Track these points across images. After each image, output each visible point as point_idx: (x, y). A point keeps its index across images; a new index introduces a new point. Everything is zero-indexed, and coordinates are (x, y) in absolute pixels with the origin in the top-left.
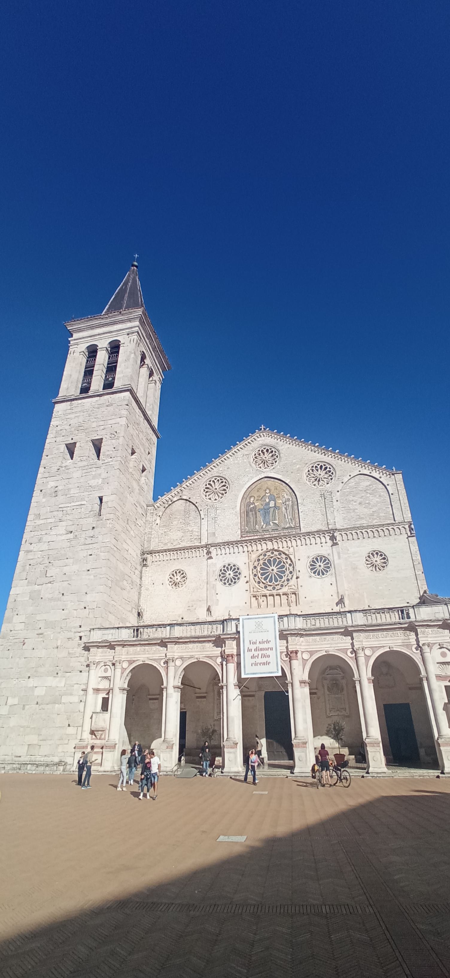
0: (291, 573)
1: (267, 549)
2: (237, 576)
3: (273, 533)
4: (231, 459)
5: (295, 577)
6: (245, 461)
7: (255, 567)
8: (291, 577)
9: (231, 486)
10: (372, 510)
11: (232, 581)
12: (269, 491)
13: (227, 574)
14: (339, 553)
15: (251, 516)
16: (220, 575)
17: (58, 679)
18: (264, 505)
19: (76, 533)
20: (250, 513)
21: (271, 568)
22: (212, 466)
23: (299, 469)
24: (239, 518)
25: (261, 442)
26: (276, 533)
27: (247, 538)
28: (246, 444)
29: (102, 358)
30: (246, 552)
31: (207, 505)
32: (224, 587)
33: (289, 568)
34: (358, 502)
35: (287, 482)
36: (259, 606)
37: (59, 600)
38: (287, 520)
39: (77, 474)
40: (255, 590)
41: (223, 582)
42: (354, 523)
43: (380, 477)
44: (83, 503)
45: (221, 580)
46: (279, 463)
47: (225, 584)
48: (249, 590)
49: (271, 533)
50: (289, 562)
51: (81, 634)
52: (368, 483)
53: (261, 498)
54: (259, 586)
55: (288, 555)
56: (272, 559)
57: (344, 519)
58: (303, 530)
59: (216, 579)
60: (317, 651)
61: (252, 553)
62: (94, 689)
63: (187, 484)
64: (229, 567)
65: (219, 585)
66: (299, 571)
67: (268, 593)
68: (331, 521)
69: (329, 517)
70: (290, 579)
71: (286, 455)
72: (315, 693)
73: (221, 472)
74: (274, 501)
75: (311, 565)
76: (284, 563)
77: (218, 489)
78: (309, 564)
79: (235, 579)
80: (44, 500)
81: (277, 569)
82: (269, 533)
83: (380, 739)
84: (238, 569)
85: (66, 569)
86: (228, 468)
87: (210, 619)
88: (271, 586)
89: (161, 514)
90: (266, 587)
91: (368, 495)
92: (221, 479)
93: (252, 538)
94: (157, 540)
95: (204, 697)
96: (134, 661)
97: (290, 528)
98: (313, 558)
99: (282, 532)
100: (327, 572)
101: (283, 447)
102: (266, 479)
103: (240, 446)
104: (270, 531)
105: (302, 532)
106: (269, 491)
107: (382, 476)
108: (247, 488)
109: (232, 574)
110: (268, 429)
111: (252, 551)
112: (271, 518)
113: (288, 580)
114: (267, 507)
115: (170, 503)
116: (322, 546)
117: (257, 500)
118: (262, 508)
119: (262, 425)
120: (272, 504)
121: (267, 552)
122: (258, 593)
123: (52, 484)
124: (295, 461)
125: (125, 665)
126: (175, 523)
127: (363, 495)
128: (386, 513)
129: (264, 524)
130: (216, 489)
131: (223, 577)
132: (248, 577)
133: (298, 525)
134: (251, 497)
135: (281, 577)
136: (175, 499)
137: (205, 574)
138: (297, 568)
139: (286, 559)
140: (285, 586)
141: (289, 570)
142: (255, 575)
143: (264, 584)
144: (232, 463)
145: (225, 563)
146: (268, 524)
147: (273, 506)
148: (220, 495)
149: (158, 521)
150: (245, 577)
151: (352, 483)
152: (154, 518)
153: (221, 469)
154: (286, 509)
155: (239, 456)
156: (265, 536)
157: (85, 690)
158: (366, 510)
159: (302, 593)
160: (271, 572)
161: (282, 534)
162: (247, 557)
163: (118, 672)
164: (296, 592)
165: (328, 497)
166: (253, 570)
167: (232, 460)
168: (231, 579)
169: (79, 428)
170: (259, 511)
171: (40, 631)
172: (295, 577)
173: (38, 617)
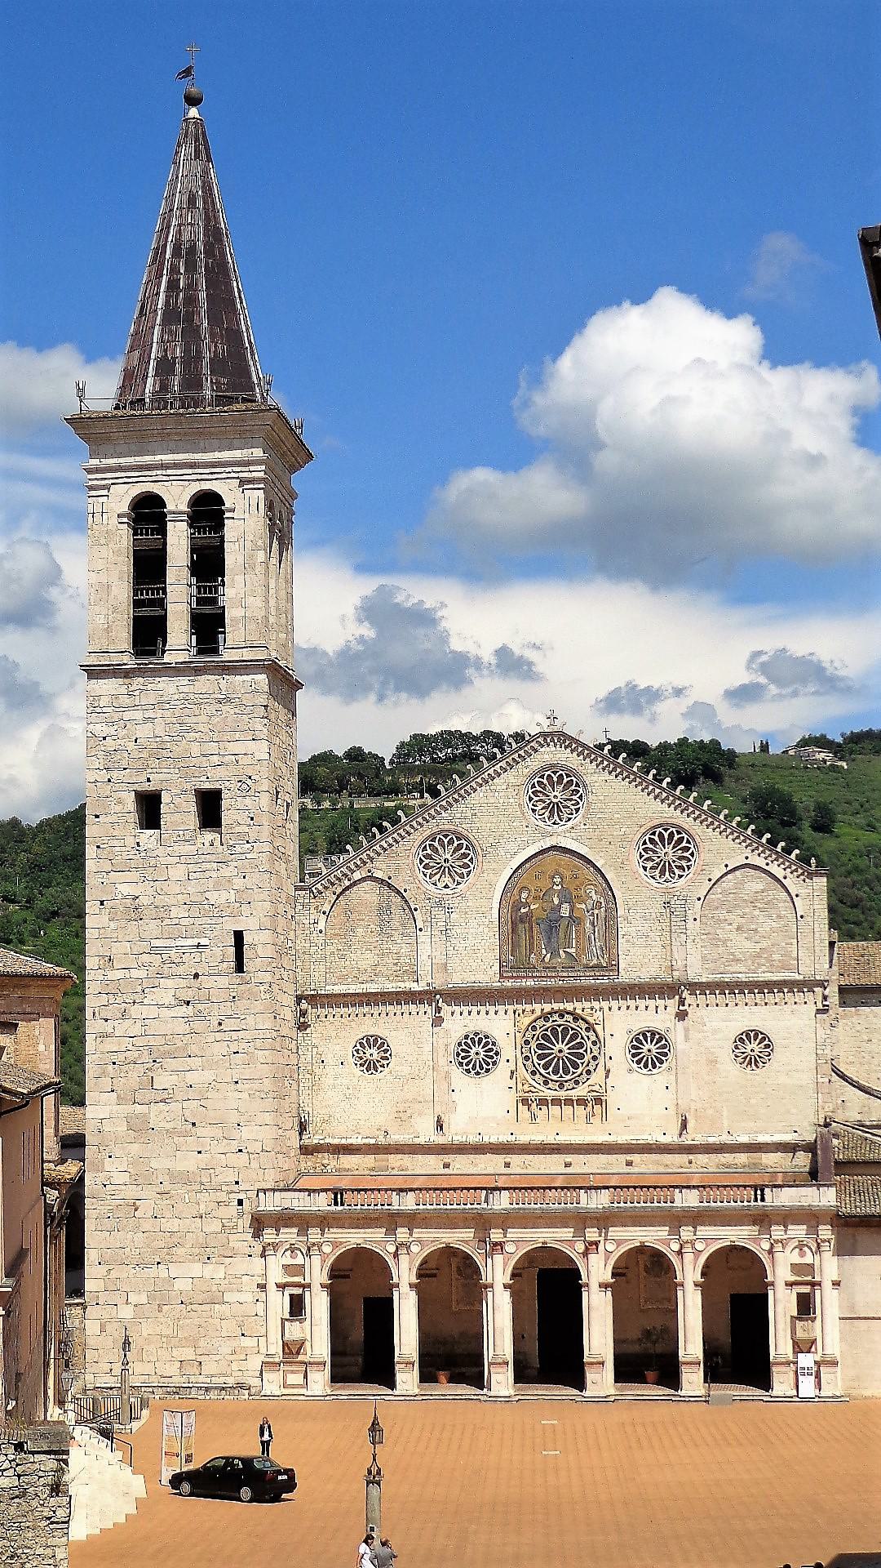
0: (595, 1058)
3: (565, 974)
4: (481, 792)
5: (601, 1071)
7: (527, 1042)
10: (759, 946)
11: (481, 1067)
12: (559, 880)
13: (473, 1051)
14: (687, 1030)
17: (210, 1267)
20: (520, 926)
32: (466, 1079)
34: (735, 925)
36: (534, 1117)
40: (526, 1088)
41: (465, 1067)
42: (721, 970)
43: (785, 878)
44: (204, 941)
45: (461, 1064)
48: (514, 1088)
50: (593, 1038)
51: (242, 1196)
52: (760, 887)
56: (559, 1030)
58: (626, 976)
59: (451, 1062)
60: (627, 1240)
62: (278, 1286)
63: (383, 843)
65: (457, 1073)
66: (611, 1058)
67: (549, 1094)
69: (676, 956)
76: (582, 1038)
77: (450, 858)
80: (113, 925)
81: (569, 1049)
83: (701, 1357)
84: (494, 1044)
85: (190, 1078)
89: (327, 908)
90: (546, 1083)
91: (757, 912)
95: (434, 1276)
96: (341, 1243)
97: (598, 966)
100: (661, 1062)
106: (559, 880)
107: (789, 875)
113: (589, 1073)
114: (554, 917)
115: (347, 883)
120: (565, 911)
122: (531, 1094)
125: (327, 1249)
127: (747, 910)
128: (786, 955)
132: (512, 1060)
133: (614, 963)
135: (576, 1067)
136: (357, 876)
137: (428, 1048)
141: (591, 1052)
142: (527, 1058)
143: (543, 1076)
145: (467, 1029)
146: (555, 954)
152: (312, 917)
154: (593, 924)
155: (499, 787)
157: (262, 1287)
158: (748, 944)
159: (612, 1099)
164: (602, 1098)
165: (679, 911)
169: (159, 751)
171: (161, 1188)
172: (601, 1068)
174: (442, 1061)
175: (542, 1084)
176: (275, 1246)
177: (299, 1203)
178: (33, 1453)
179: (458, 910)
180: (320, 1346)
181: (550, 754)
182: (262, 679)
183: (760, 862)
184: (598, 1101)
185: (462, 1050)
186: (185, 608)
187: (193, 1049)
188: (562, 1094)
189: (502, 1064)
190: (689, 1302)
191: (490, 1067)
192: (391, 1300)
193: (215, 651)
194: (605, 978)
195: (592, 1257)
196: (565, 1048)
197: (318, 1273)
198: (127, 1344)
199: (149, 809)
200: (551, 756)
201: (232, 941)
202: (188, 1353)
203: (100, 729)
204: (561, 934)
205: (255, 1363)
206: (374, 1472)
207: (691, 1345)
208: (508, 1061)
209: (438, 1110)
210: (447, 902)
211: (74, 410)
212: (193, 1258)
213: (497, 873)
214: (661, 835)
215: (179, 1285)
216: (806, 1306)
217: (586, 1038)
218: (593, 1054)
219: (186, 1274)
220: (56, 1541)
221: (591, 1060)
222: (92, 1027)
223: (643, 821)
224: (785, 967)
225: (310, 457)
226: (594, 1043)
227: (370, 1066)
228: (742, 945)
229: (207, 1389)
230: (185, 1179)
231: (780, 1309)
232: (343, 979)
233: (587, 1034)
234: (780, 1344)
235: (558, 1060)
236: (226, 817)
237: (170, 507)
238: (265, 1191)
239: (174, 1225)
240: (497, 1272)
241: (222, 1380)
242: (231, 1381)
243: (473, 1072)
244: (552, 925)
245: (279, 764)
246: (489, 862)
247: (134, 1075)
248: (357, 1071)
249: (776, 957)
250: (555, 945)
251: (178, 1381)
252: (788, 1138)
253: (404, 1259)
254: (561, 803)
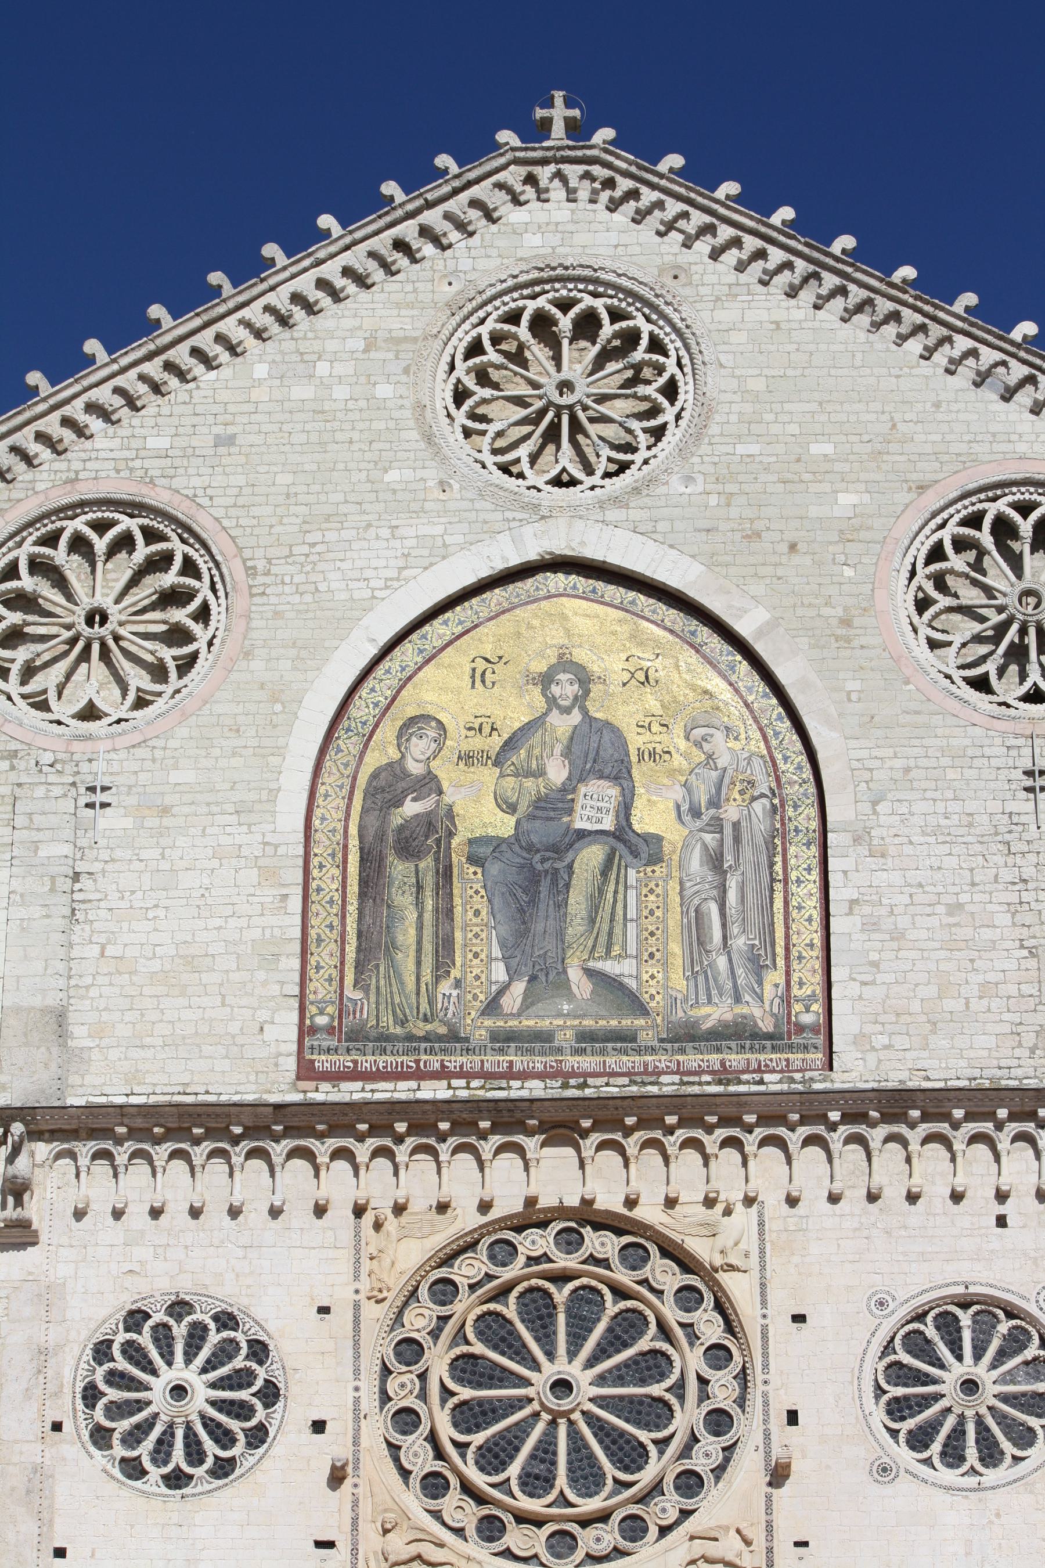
1: (531, 1202)
2: (242, 1411)
3: (587, 1062)
6: (384, 390)
8: (718, 1458)
9: (239, 602)
11: (195, 1453)
13: (159, 1387)
16: (91, 1395)
18: (523, 808)
20: (399, 869)
21: (551, 1371)
22: (79, 403)
24: (295, 904)
25: (533, 240)
26: (612, 1062)
27: (351, 1092)
28: (400, 245)
30: (340, 1214)
31: (14, 754)
33: (703, 1381)
35: (743, 628)
38: (722, 962)
41: (119, 1451)
45: (101, 1437)
46: (682, 451)
47: (133, 1469)
48: (343, 1546)
49: (572, 1062)
50: (712, 1330)
53: (511, 744)
54: (437, 1515)
55: (707, 1274)
56: (561, 1295)
59: (57, 1427)
61: (391, 1224)
64: (180, 1331)
66: (793, 1417)
70: (708, 1478)
71: (757, 385)
73: (155, 466)
74: (616, 779)
75: (898, 1373)
76: (664, 1331)
78: (874, 1366)
79: (224, 1438)
82: (550, 1060)
84: (259, 1350)
86: (219, 441)
88: (538, 1522)
92: (151, 536)
93: (403, 1091)
98: (920, 1317)
99: (661, 1061)
101: (727, 315)
102: (558, 581)
103: (346, 259)
104: (565, 1038)
105: (840, 1080)
108: (385, 637)
110: (605, 134)
111: (399, 1209)
112: (576, 928)
116: (1001, 1221)
117: (467, 758)
118: (504, 826)
119: (559, 96)
121: (519, 1229)
124: (828, 449)
129: (513, 974)
130: (97, 616)
131: (116, 1410)
132: (338, 1428)
133: (807, 1019)
139: (688, 1298)
140: (664, 1531)
141: (704, 1396)
143: (480, 1499)
144: (259, 394)
147: (608, 824)
148: (138, 679)
150: (319, 1427)
153: (158, 443)
154: (715, 861)
155: (332, 345)
156: (517, 1090)
160: (552, 1402)
161: (669, 1084)
162: (346, 1256)
166: (386, 1371)
167: (261, 370)
168: (190, 1433)
170: (472, 860)
175: (471, 1531)
179: (132, 800)
185: (115, 1378)
191: (236, 1451)
194: (767, 1077)
200: (555, 239)
208: (319, 1427)
210: (85, 767)
217: (679, 1332)
218: (707, 1406)
221: (701, 1431)
226: (718, 1355)
233: (686, 1318)
235: (553, 1423)
243: (155, 1473)
246: (277, 615)
250: (550, 944)
254: (585, 408)
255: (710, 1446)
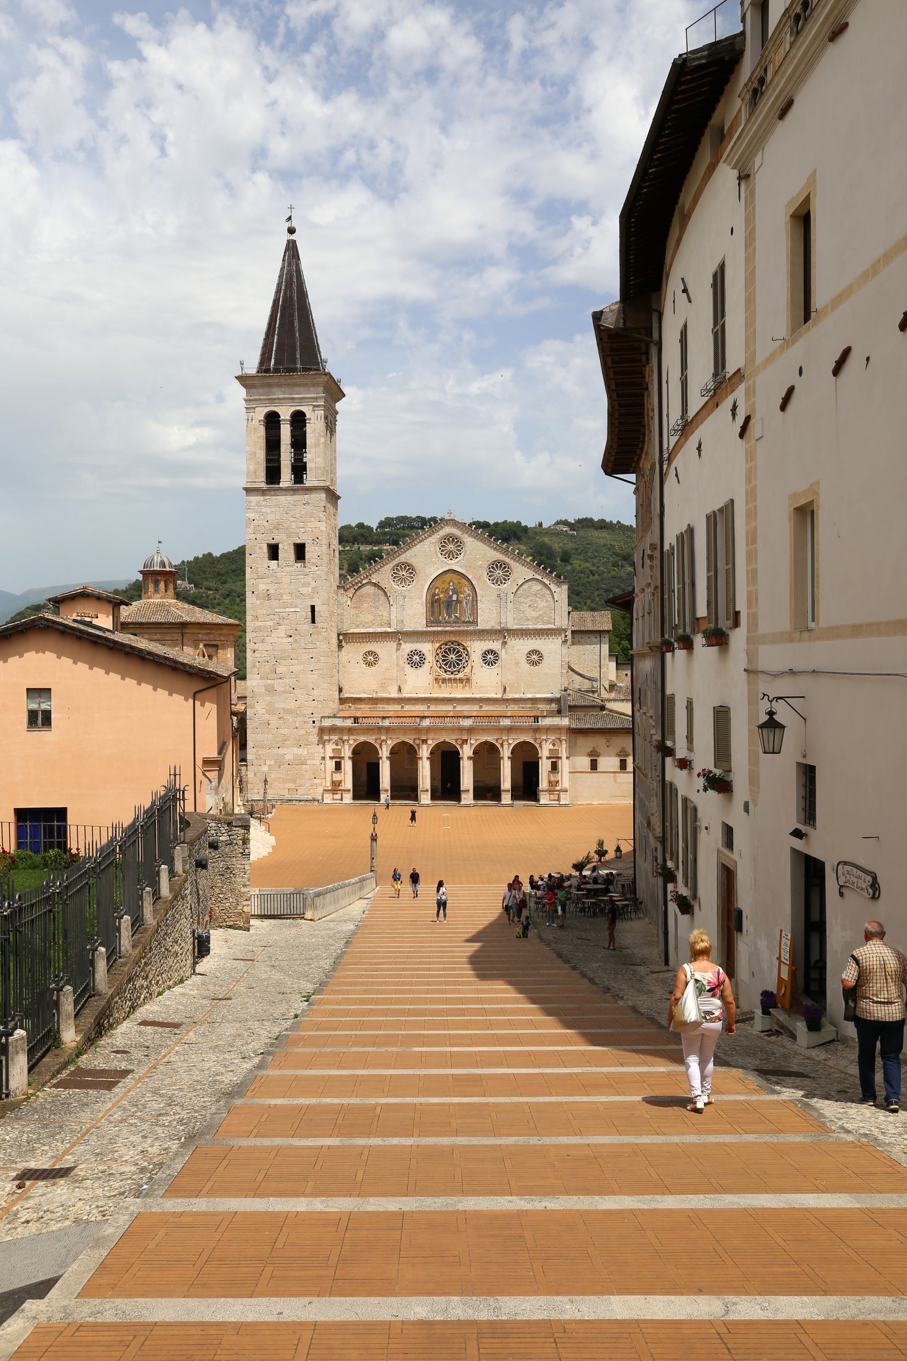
0: (467, 661)
7: (438, 654)
15: (435, 607)
19: (296, 638)
20: (435, 604)
23: (480, 566)
29: (286, 432)
37: (291, 693)
39: (286, 580)
44: (298, 610)
57: (514, 619)
67: (446, 676)
68: (503, 621)
72: (477, 753)
80: (258, 602)
85: (292, 668)
87: (400, 696)
90: (446, 672)
94: (349, 622)
97: (469, 622)
109: (418, 659)
113: (464, 667)
114: (449, 600)
118: (446, 599)
120: (455, 597)
123: (262, 587)
126: (366, 605)
130: (403, 575)
134: (436, 588)
136: (364, 582)
137: (395, 657)
138: (472, 658)
142: (437, 661)
146: (450, 616)
149: (349, 603)
151: (526, 586)
158: (534, 613)
159: (474, 679)
163: (347, 747)
172: (469, 665)
173: (276, 706)
174: (401, 662)
176: (329, 741)
177: (339, 723)
178: (236, 827)
180: (348, 784)
181: (448, 530)
182: (323, 496)
183: (540, 578)
184: (468, 679)
186: (289, 463)
187: (293, 656)
188: (452, 676)
189: (426, 663)
190: (506, 765)
192: (378, 764)
193: (302, 482)
195: (465, 746)
196: (454, 657)
197: (347, 752)
198: (266, 781)
199: (273, 552)
201: (310, 610)
202: (292, 786)
203: (252, 515)
204: (453, 608)
205: (321, 790)
206: (374, 834)
207: (506, 783)
209: (399, 683)
211: (239, 373)
212: (294, 745)
213: (425, 581)
214: (497, 565)
215: (287, 757)
216: (554, 767)
219: (290, 753)
220: (245, 862)
222: (249, 647)
223: (488, 559)
224: (549, 623)
225: (344, 395)
227: (369, 664)
228: (531, 613)
229: (300, 801)
230: (290, 712)
231: (544, 768)
232: (357, 626)
234: (543, 784)
236: (307, 555)
237: (282, 418)
238: (324, 717)
239: (286, 731)
240: (424, 752)
241: (306, 797)
242: (310, 798)
244: (449, 605)
245: (330, 532)
247: (268, 668)
248: (364, 666)
249: (546, 618)
251: (288, 797)
252: (549, 696)
253: (384, 747)
255: (466, 663)
